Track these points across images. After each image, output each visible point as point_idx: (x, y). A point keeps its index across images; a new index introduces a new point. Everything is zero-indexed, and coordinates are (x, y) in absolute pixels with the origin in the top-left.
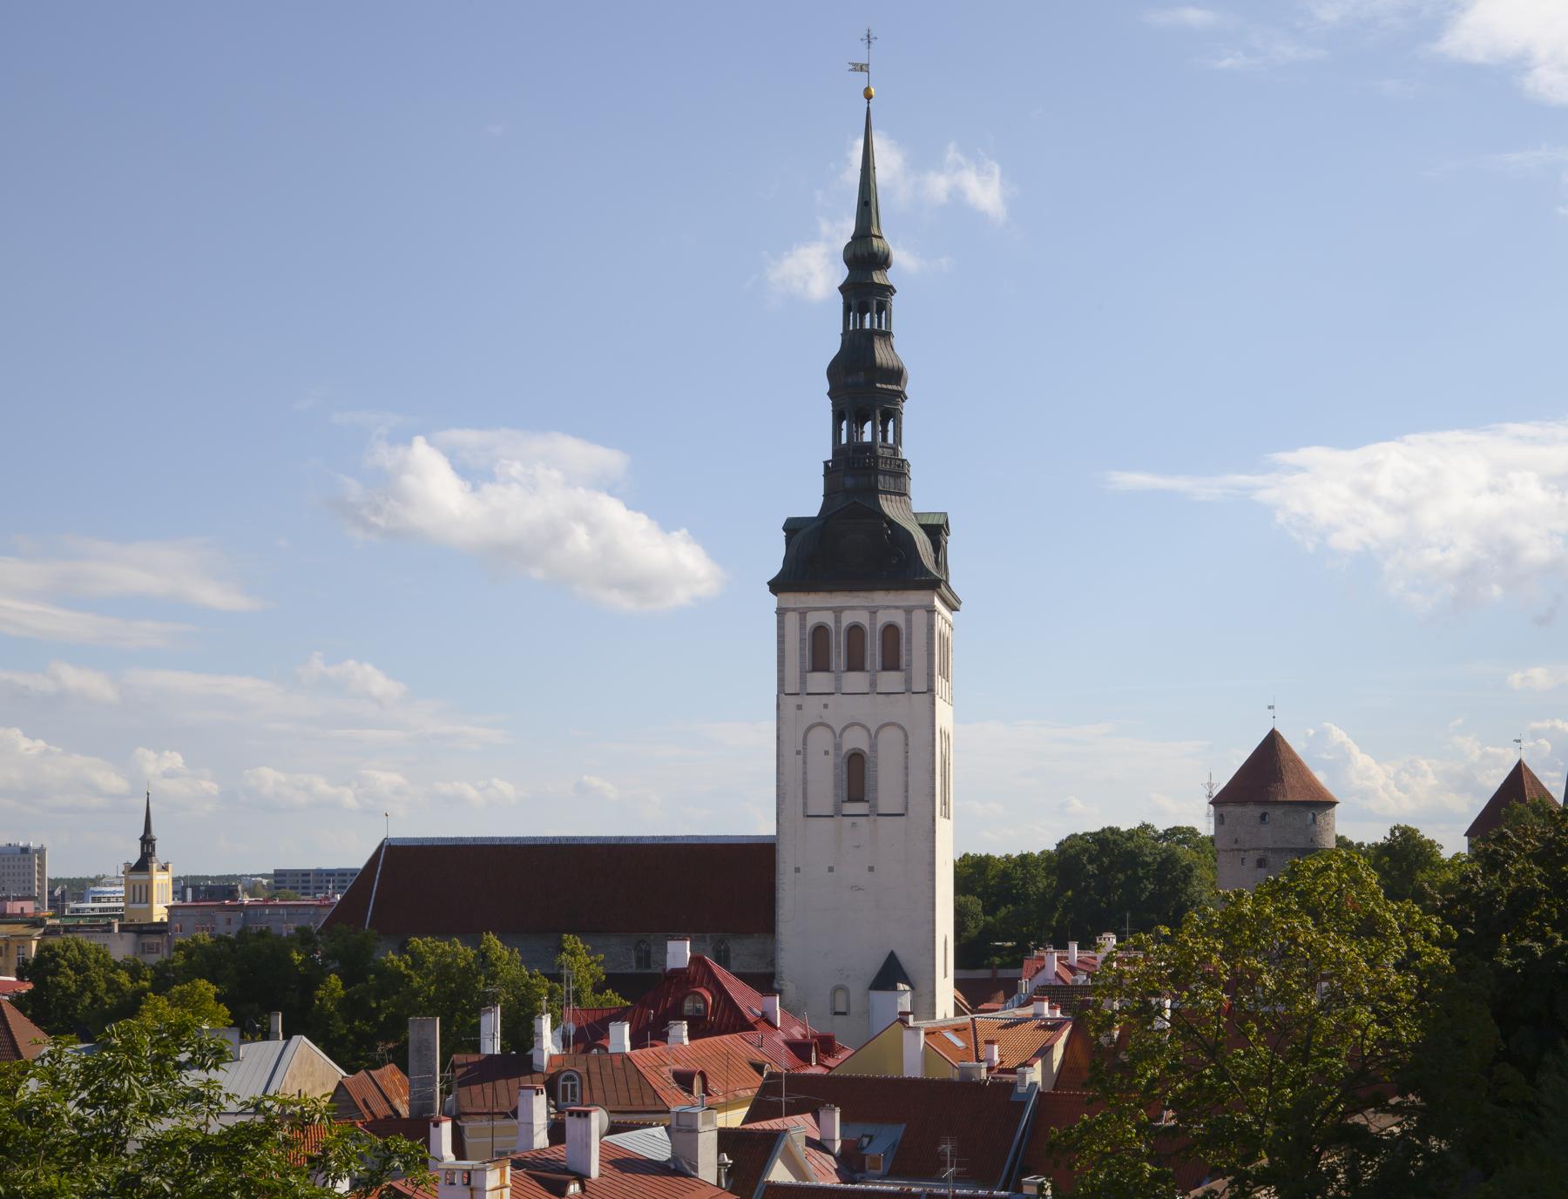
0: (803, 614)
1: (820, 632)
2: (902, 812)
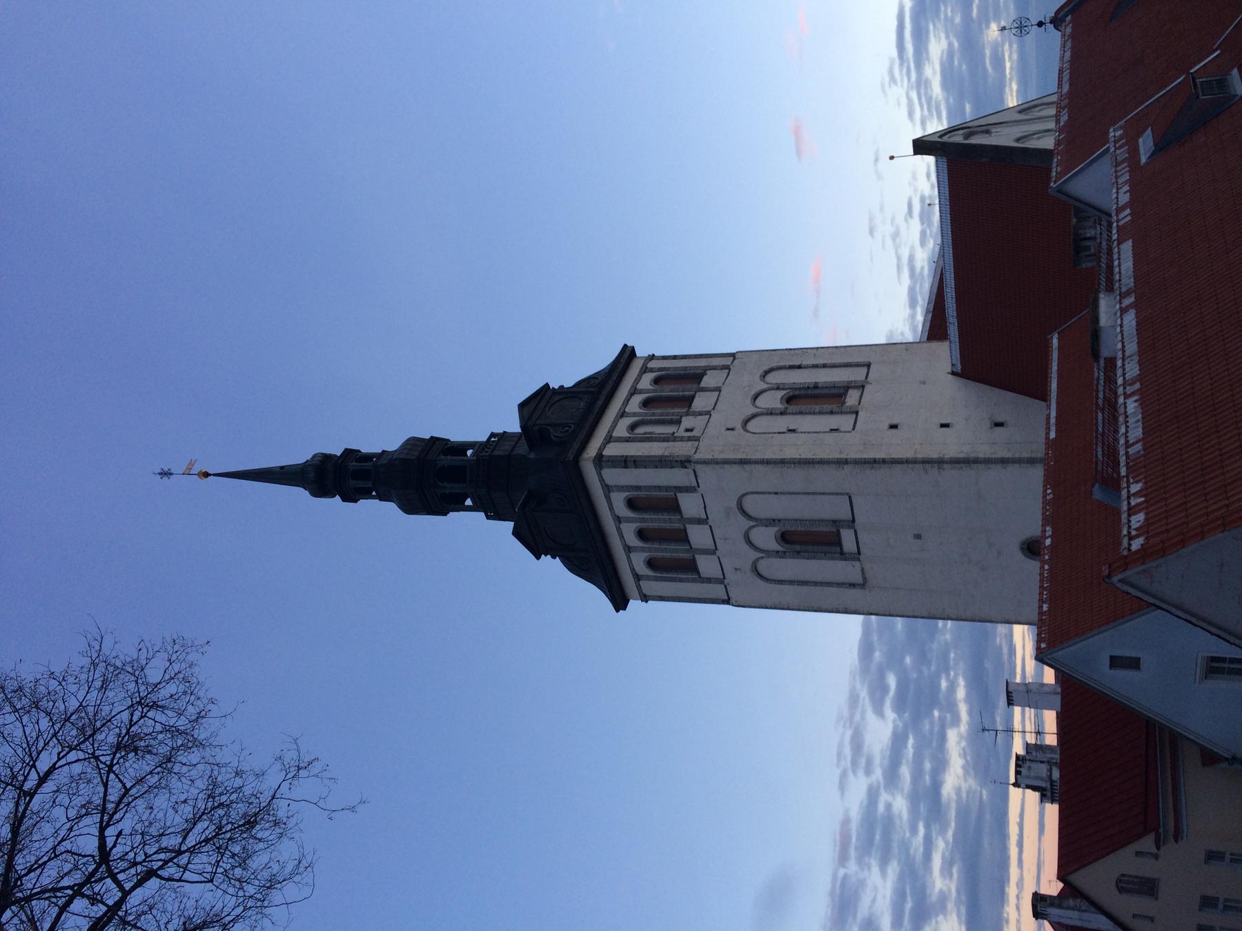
0: (638, 578)
1: (651, 564)
2: (848, 497)
